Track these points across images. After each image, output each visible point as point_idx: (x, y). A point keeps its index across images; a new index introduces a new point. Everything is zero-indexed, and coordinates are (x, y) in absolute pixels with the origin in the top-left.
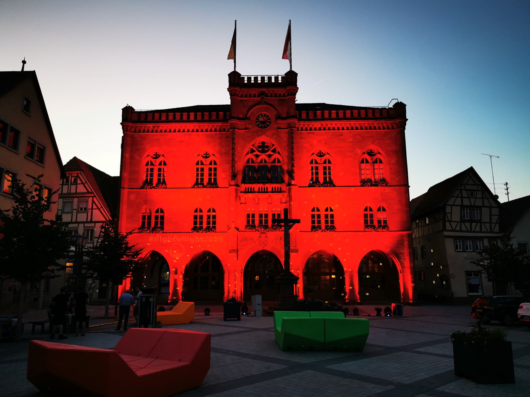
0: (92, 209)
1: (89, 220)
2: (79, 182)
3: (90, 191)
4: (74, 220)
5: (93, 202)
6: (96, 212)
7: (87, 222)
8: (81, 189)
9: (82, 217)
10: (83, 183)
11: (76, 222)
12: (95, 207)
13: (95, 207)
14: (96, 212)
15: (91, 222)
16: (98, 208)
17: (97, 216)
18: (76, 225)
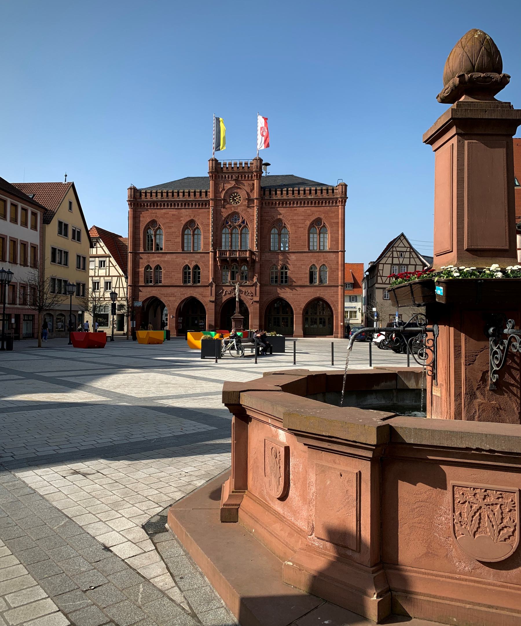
0: (109, 266)
1: (107, 275)
2: (98, 245)
3: (107, 253)
4: (96, 275)
5: (110, 261)
6: (112, 269)
7: (106, 276)
8: (100, 252)
9: (102, 272)
10: (101, 247)
11: (98, 276)
12: (111, 265)
13: (111, 265)
14: (112, 269)
15: (109, 276)
16: (114, 266)
17: (113, 272)
18: (98, 278)
